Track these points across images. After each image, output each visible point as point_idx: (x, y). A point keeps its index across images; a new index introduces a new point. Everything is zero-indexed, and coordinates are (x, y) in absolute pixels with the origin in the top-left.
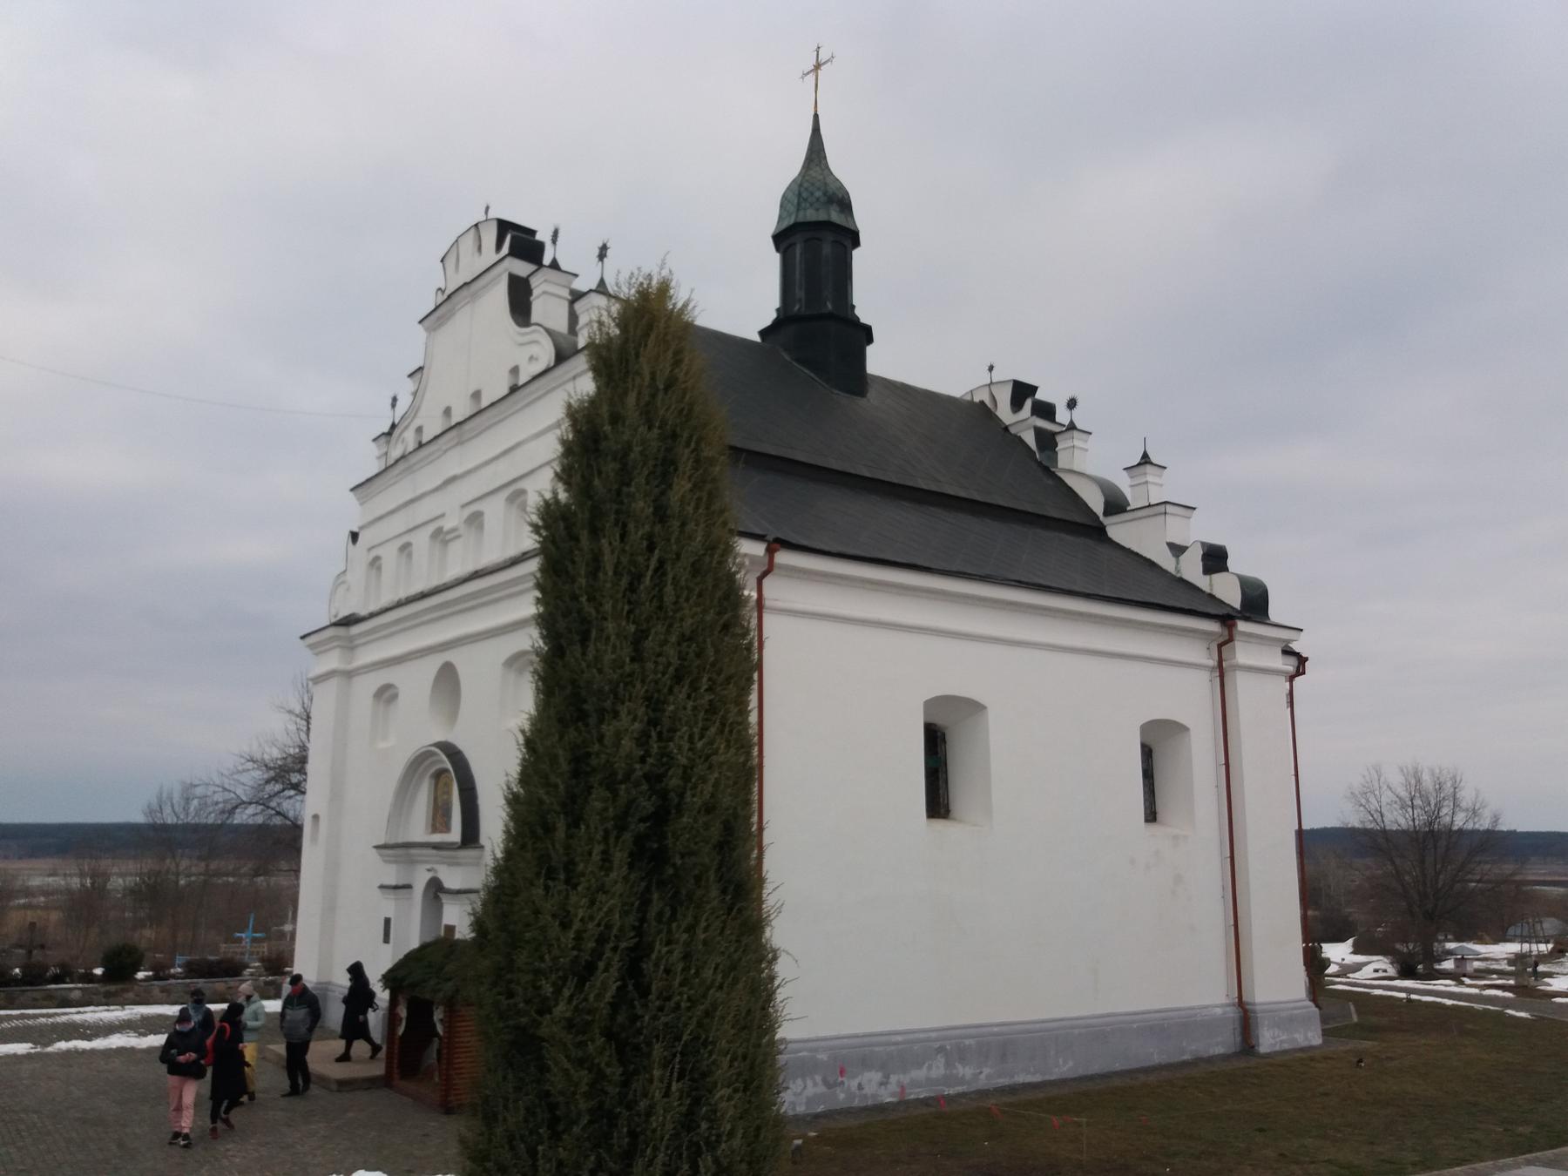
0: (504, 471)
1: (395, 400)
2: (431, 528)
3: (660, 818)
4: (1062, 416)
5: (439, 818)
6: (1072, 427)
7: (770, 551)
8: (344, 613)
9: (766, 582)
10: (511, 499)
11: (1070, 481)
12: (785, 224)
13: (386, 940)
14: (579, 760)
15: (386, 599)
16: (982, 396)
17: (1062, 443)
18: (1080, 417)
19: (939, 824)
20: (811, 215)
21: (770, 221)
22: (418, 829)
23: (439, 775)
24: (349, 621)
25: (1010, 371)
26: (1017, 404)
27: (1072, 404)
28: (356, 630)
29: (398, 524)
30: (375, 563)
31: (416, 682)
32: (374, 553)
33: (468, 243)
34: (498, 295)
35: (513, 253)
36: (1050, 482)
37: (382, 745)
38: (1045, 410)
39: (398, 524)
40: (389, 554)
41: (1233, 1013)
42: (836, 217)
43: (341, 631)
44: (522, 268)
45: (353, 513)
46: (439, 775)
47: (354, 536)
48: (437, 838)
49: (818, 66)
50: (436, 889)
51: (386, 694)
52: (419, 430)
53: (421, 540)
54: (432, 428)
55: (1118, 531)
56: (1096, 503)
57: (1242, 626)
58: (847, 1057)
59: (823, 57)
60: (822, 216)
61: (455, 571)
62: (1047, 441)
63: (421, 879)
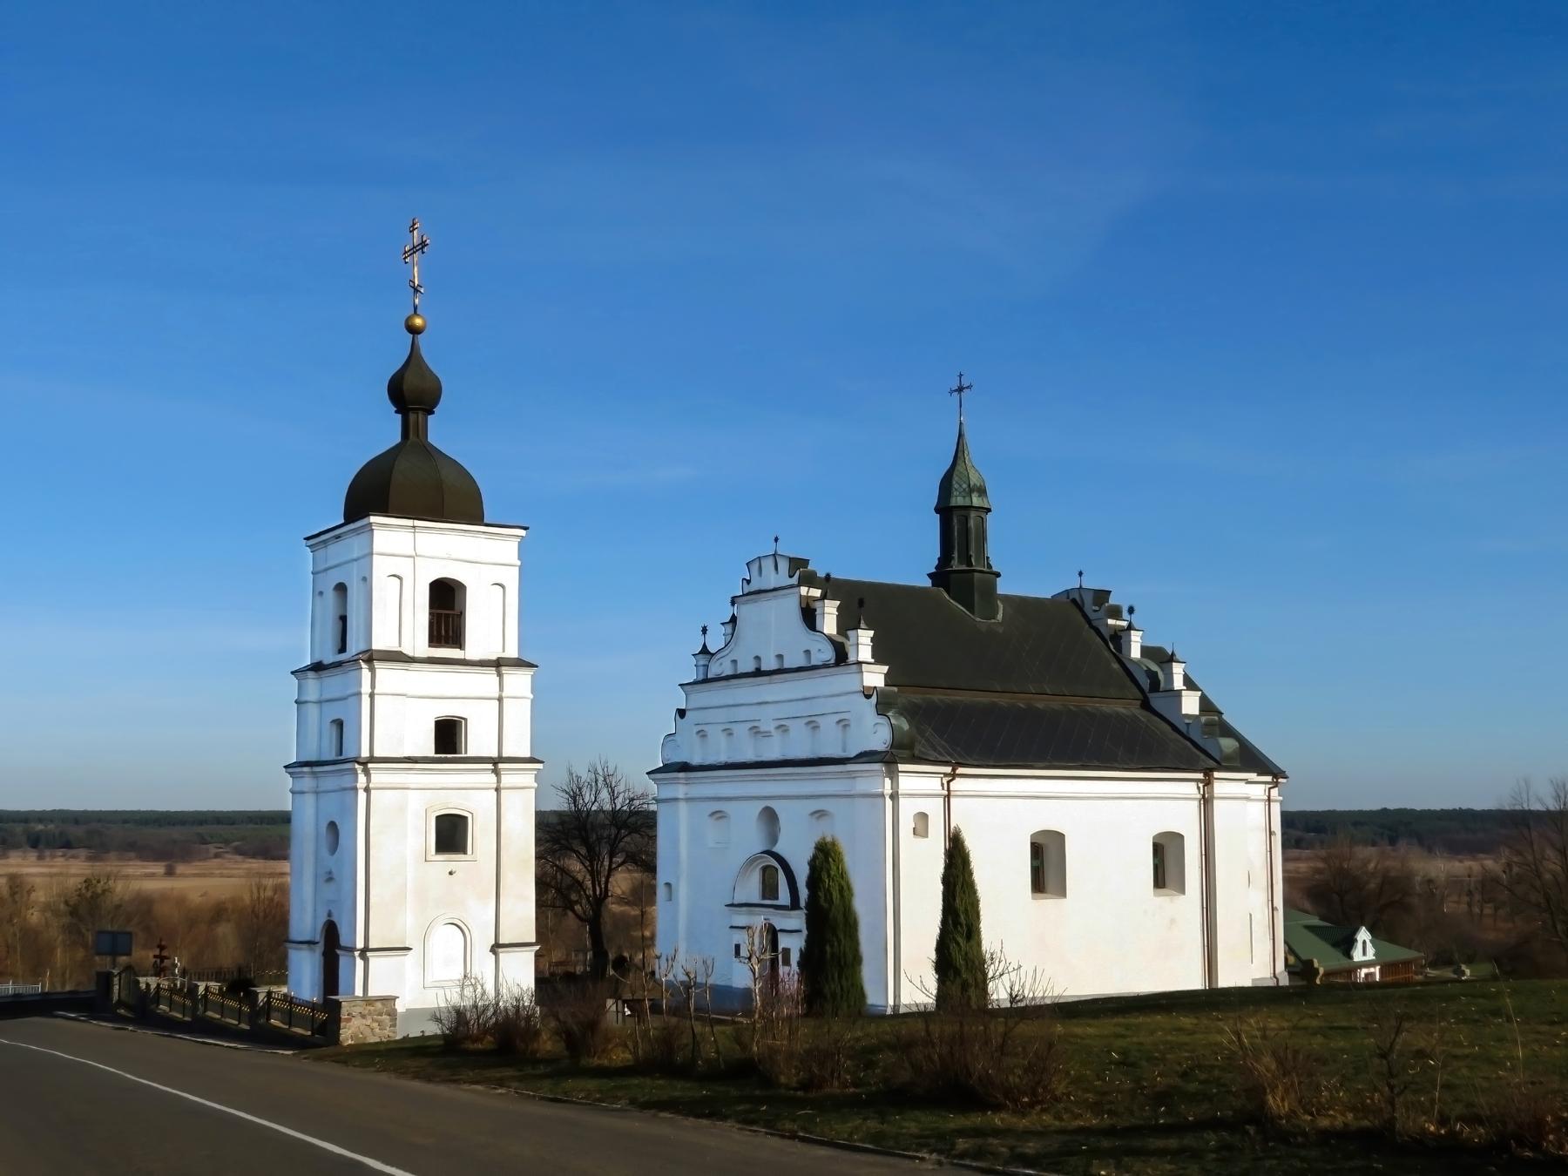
1: (704, 630)
2: (750, 725)
4: (1125, 614)
5: (769, 890)
18: (1135, 619)
24: (685, 767)
25: (1092, 583)
27: (1131, 610)
29: (721, 716)
30: (702, 734)
33: (768, 565)
38: (1116, 612)
43: (682, 775)
46: (765, 869)
47: (681, 713)
49: (960, 389)
52: (734, 662)
53: (741, 731)
57: (1216, 774)
59: (965, 384)
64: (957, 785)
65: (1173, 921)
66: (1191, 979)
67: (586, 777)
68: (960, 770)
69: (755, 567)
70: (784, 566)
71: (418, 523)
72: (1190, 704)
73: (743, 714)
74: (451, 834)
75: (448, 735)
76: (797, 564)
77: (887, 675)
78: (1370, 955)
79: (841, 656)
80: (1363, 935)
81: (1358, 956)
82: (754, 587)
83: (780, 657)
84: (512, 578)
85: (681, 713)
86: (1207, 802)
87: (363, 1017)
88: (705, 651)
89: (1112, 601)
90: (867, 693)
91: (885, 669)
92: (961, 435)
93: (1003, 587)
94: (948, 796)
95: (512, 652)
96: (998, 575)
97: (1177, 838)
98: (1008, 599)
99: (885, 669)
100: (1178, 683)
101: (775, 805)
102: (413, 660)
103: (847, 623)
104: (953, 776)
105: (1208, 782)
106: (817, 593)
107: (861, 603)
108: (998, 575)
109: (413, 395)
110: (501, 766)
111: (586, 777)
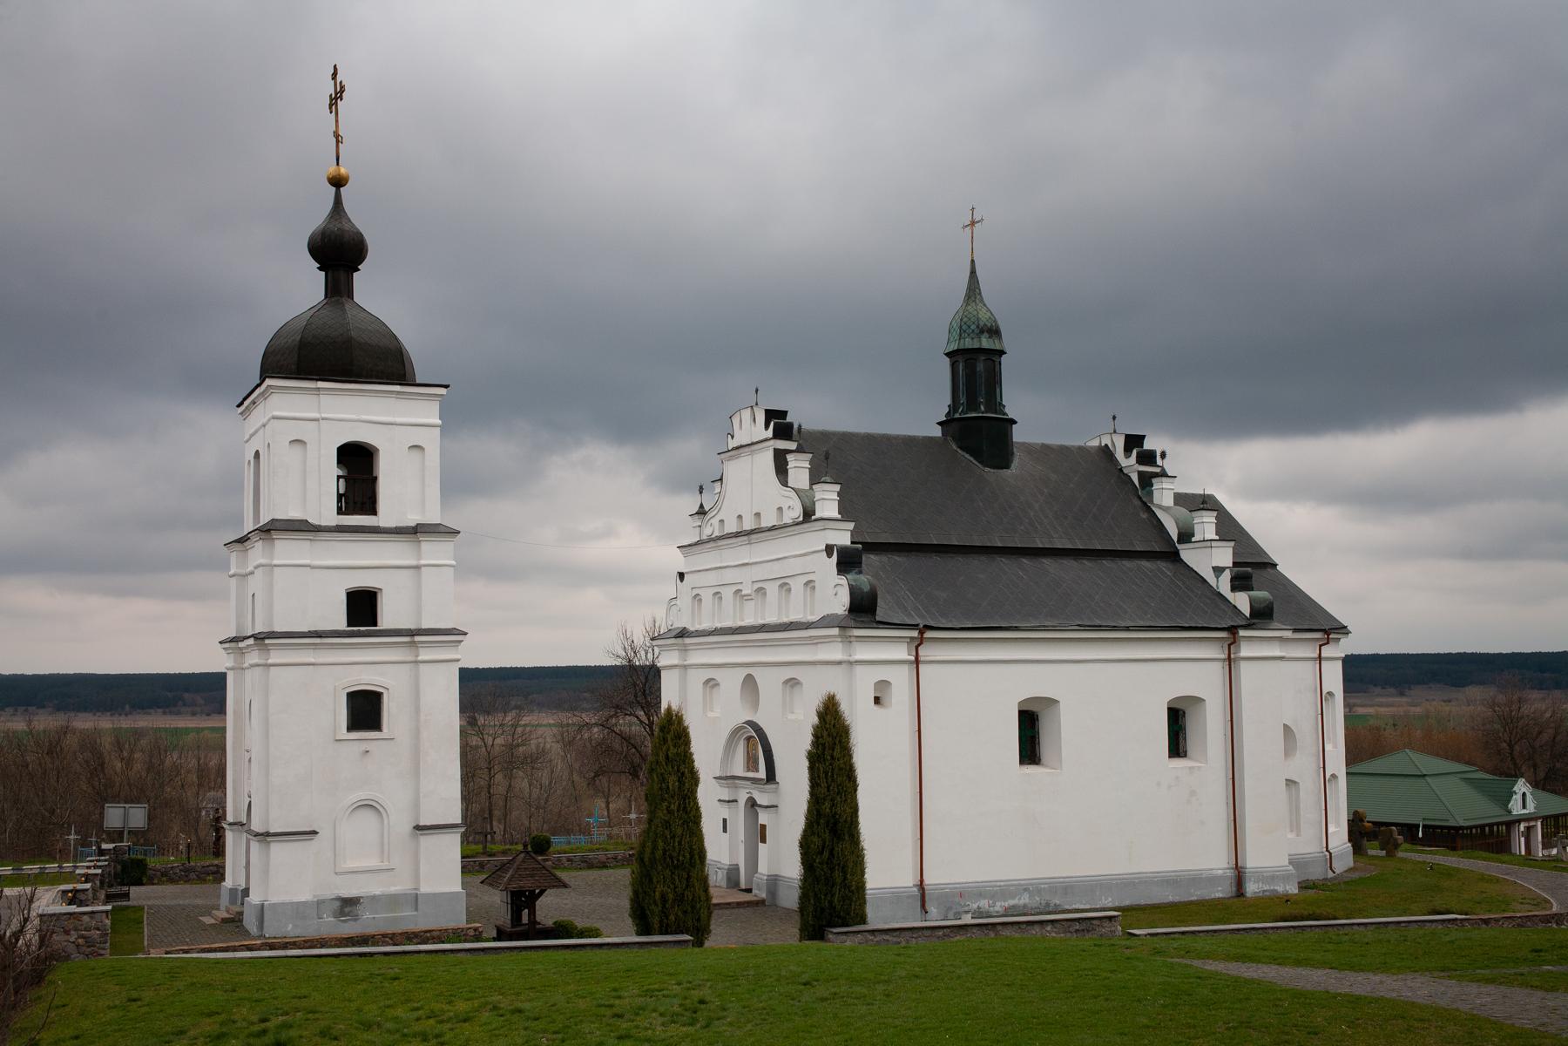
0: (777, 570)
2: (735, 588)
3: (835, 824)
5: (751, 763)
6: (1163, 474)
7: (921, 633)
8: (679, 624)
9: (922, 651)
10: (781, 586)
11: (1159, 514)
12: (953, 347)
13: (725, 830)
14: (819, 814)
15: (706, 625)
16: (1106, 441)
17: (1157, 484)
18: (1168, 465)
19: (1031, 770)
20: (969, 343)
21: (941, 340)
22: (739, 768)
23: (749, 739)
24: (683, 633)
26: (1128, 450)
27: (1163, 455)
28: (688, 641)
29: (712, 579)
31: (731, 682)
32: (696, 592)
34: (768, 457)
35: (776, 436)
36: (1144, 516)
37: (710, 714)
38: (1148, 458)
39: (712, 579)
40: (707, 596)
41: (1230, 873)
42: (986, 343)
43: (679, 641)
44: (783, 444)
45: (679, 562)
46: (749, 739)
47: (681, 576)
48: (751, 775)
49: (973, 223)
50: (752, 804)
51: (711, 684)
53: (728, 593)
54: (731, 527)
55: (1188, 554)
56: (1174, 534)
57: (1242, 633)
58: (962, 893)
60: (976, 346)
61: (749, 621)
62: (1146, 480)
63: (743, 797)
64: (925, 652)
65: (1193, 793)
66: (1216, 861)
67: (640, 638)
68: (928, 634)
69: (736, 421)
70: (761, 417)
71: (321, 384)
72: (1224, 556)
73: (729, 576)
74: (365, 711)
75: (362, 606)
76: (771, 415)
77: (852, 532)
78: (1531, 807)
79: (808, 514)
80: (1521, 786)
81: (1516, 808)
82: (732, 444)
83: (758, 515)
84: (431, 441)
85: (681, 576)
86: (1230, 661)
87: (67, 932)
88: (702, 512)
89: (1147, 445)
90: (829, 550)
91: (851, 526)
92: (973, 272)
93: (1019, 435)
94: (917, 661)
95: (433, 516)
96: (1013, 422)
97: (1197, 701)
98: (1029, 448)
99: (851, 526)
100: (1211, 533)
101: (758, 673)
102: (318, 529)
103: (815, 479)
104: (921, 641)
105: (1233, 642)
106: (792, 446)
107: (834, 456)
108: (1013, 422)
109: (338, 253)
110: (417, 638)
111: (640, 638)
